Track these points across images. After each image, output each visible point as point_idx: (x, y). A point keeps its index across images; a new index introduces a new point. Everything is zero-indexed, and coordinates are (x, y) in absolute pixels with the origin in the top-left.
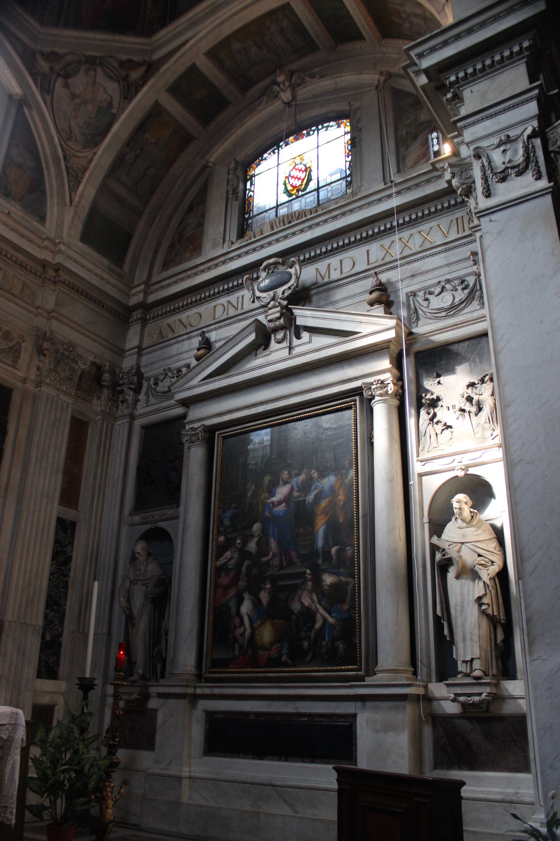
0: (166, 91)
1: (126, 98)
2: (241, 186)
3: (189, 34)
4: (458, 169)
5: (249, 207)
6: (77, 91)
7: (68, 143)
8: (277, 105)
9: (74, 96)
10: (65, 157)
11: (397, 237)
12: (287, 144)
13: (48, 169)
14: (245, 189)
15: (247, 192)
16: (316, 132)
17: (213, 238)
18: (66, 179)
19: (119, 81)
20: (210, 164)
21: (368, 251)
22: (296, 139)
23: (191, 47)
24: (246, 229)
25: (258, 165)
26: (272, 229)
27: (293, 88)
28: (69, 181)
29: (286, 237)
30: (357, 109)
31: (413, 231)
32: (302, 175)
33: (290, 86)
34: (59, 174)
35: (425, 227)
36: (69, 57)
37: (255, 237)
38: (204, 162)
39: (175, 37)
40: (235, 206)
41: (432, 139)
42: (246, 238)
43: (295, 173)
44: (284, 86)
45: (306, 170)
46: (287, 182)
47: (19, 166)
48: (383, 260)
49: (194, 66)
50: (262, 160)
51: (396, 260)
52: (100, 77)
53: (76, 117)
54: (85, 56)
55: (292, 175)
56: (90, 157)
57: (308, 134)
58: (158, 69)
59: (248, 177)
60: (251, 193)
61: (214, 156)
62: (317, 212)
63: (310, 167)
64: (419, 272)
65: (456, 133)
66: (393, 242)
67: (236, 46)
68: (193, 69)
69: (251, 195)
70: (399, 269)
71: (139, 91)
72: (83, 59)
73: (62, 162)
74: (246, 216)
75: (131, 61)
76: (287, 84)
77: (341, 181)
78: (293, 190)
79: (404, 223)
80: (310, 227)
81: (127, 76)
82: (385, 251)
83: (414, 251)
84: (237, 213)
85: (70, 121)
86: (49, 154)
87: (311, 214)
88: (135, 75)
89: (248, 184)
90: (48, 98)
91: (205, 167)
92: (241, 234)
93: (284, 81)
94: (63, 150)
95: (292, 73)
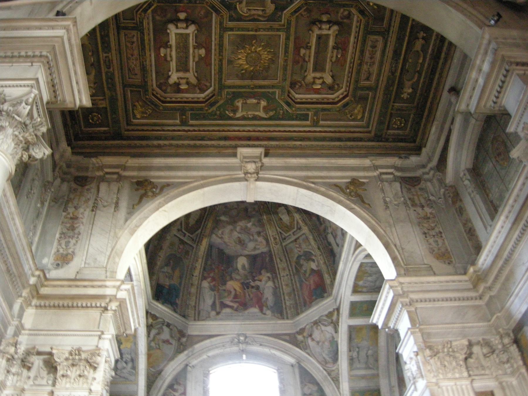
6: (318, 340)
7: (328, 365)
9: (318, 343)
18: (333, 384)
52: (323, 328)
53: (324, 351)
54: (312, 323)
67: (361, 283)
72: (312, 324)
81: (332, 320)
85: (322, 354)
88: (335, 318)
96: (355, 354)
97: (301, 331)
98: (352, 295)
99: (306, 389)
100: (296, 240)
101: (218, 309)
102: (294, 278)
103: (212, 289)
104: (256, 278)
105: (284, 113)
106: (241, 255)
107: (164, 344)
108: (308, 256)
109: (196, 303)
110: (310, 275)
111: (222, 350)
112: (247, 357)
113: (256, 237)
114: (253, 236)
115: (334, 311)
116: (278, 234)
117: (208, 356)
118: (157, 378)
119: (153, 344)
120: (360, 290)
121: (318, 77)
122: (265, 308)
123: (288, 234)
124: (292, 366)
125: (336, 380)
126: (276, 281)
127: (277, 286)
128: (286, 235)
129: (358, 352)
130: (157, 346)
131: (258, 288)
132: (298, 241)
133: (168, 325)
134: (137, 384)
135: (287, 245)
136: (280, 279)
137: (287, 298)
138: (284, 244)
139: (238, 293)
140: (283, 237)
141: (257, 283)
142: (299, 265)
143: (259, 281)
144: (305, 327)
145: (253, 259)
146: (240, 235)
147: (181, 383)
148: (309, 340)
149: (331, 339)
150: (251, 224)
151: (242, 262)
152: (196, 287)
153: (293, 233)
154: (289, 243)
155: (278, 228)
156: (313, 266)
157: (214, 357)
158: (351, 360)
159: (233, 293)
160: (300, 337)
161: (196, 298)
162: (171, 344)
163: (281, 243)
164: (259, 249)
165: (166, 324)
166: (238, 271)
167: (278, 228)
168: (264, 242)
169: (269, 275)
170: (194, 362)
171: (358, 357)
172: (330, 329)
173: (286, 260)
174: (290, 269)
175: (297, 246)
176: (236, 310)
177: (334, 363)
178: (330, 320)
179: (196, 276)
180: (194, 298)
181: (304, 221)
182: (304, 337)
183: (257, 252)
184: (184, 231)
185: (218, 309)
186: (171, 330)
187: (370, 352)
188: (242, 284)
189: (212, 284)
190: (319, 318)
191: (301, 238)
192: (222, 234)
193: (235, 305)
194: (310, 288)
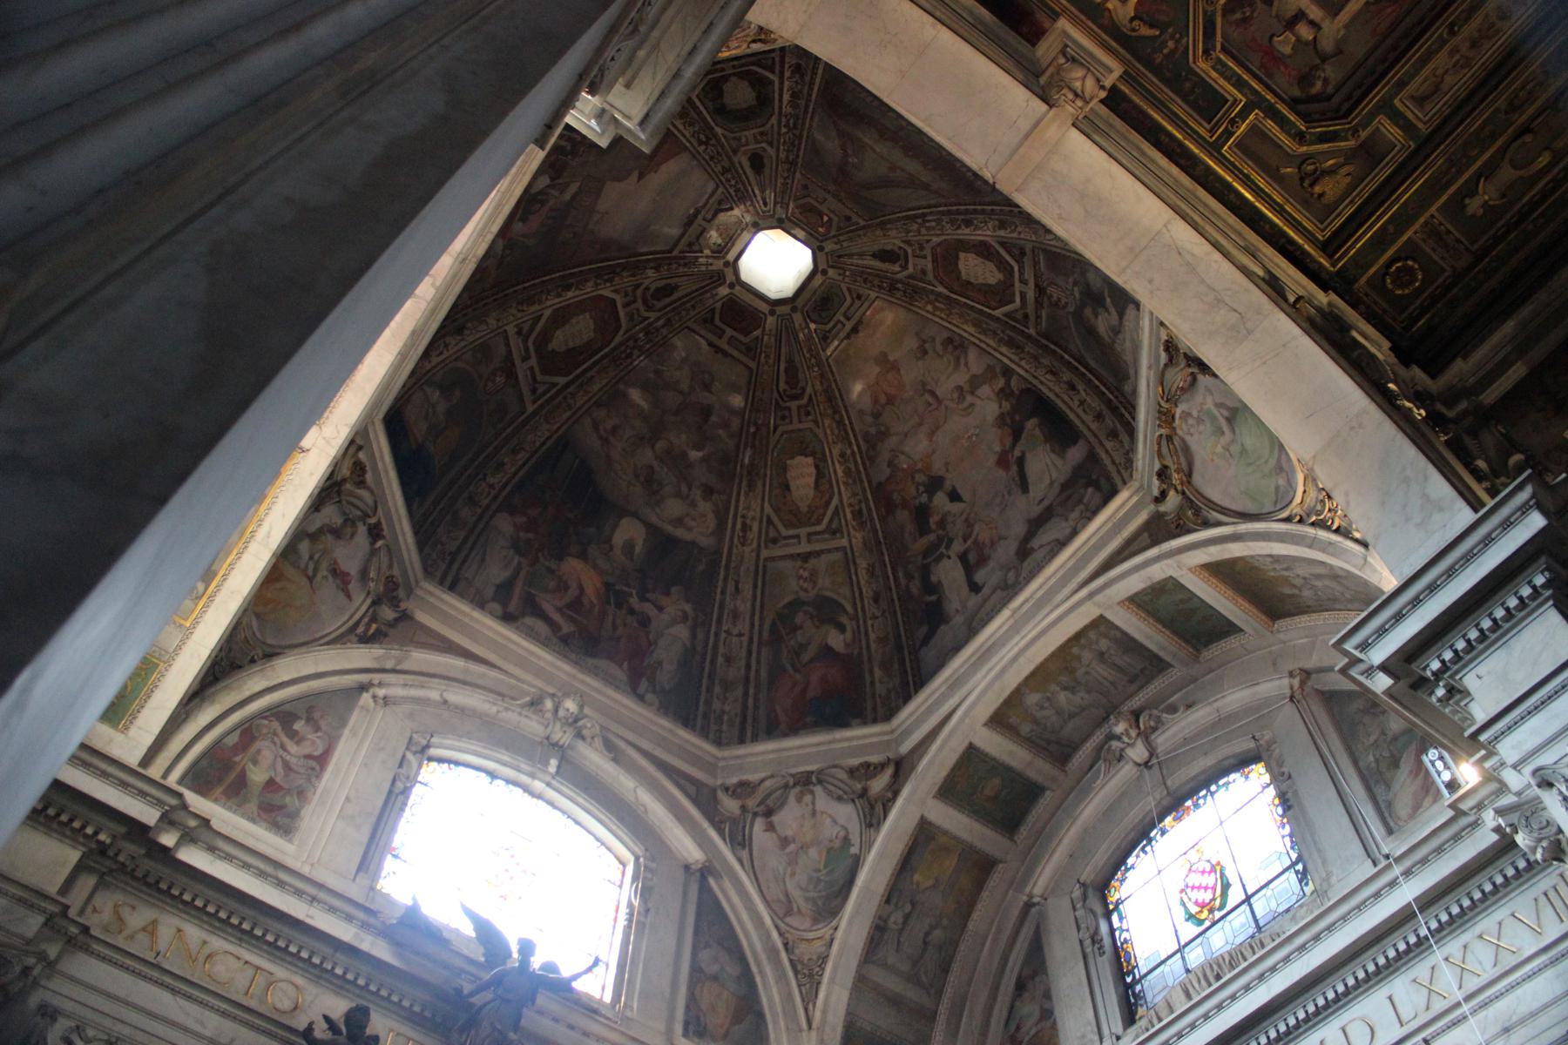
0: (934, 797)
1: (870, 825)
2: (1104, 927)
3: (952, 702)
4: (1518, 814)
5: (1128, 962)
6: (789, 833)
7: (788, 920)
8: (1126, 771)
9: (785, 842)
10: (786, 945)
11: (1437, 955)
12: (1163, 832)
13: (761, 972)
14: (1112, 931)
15: (1117, 933)
16: (1209, 798)
17: (1079, 1034)
19: (853, 801)
20: (1036, 900)
21: (1390, 998)
22: (1178, 819)
23: (961, 720)
24: (1136, 1004)
25: (1122, 881)
26: (1189, 996)
27: (1146, 736)
28: (799, 986)
29: (1220, 1007)
30: (1270, 744)
31: (1466, 937)
32: (1210, 880)
33: (1138, 735)
34: (781, 978)
35: (1487, 923)
36: (768, 783)
37: (1160, 1020)
38: (1025, 898)
39: (930, 711)
40: (1104, 966)
41: (1433, 763)
42: (1143, 1023)
43: (1196, 879)
44: (1130, 737)
45: (1213, 870)
46: (1186, 900)
47: (715, 978)
48: (1428, 1008)
49: (971, 747)
50: (1127, 870)
51: (1458, 1005)
53: (793, 874)
54: (792, 775)
55: (1190, 884)
56: (827, 937)
57: (1196, 806)
58: (913, 768)
59: (1111, 907)
60: (1125, 935)
61: (1040, 884)
62: (1263, 946)
63: (1218, 863)
64: (1515, 1019)
65: (1483, 752)
66: (1433, 968)
67: (1032, 699)
68: (972, 753)
69: (1125, 940)
70: (1472, 1020)
71: (890, 808)
72: (791, 782)
73: (784, 955)
74: (1129, 980)
75: (867, 765)
76: (1133, 733)
77: (1287, 874)
78: (1201, 912)
79: (1441, 927)
80: (1261, 977)
82: (1425, 991)
83: (1486, 978)
84: (1110, 978)
85: (784, 882)
86: (759, 946)
87: (1254, 953)
88: (878, 784)
89: (1115, 917)
90: (745, 854)
91: (1029, 906)
92: (1130, 1018)
93: (1126, 730)
94: (781, 934)
95: (1136, 715)
96: (897, 917)
97: (742, 789)
98: (985, 724)
99: (705, 955)
100: (806, 557)
101: (513, 606)
102: (759, 653)
103: (516, 545)
104: (648, 595)
105: (1173, 52)
106: (635, 515)
107: (331, 579)
108: (827, 612)
109: (459, 549)
110: (811, 661)
111: (494, 709)
112: (559, 767)
113: (697, 494)
114: (690, 489)
115: (882, 766)
116: (761, 521)
117: (445, 702)
118: (253, 661)
119: (304, 547)
120: (1013, 720)
121: (1312, 16)
122: (644, 684)
123: (792, 532)
124: (687, 868)
125: (809, 975)
126: (700, 636)
127: (699, 649)
128: (784, 532)
129: (907, 917)
130: (311, 566)
131: (645, 622)
132: (813, 562)
133: (375, 533)
134: (188, 633)
135: (773, 559)
136: (717, 635)
137: (717, 689)
138: (765, 553)
139: (585, 601)
140: (772, 534)
141: (649, 609)
142: (784, 622)
143: (656, 606)
144: (762, 781)
145: (662, 544)
146: (655, 464)
147: (323, 723)
148: (759, 825)
149: (837, 844)
150: (700, 454)
151: (629, 532)
152: (479, 511)
153: (809, 534)
154: (782, 558)
155: (766, 504)
156: (836, 640)
157: (462, 711)
158: (879, 930)
159: (573, 592)
160: (730, 805)
161: (466, 538)
162: (349, 597)
163: (759, 546)
164: (690, 529)
165: (373, 521)
166: (611, 548)
167: (766, 504)
168: (711, 522)
169: (688, 607)
170: (395, 688)
171: (901, 932)
172: (846, 815)
173: (754, 596)
174: (757, 623)
175: (806, 574)
176: (565, 640)
177: (816, 921)
178: (858, 787)
179: (491, 486)
180: (462, 535)
181: (857, 514)
182: (743, 808)
183: (680, 533)
184: (530, 344)
185: (513, 606)
186: (374, 552)
187: (937, 934)
188: (607, 586)
189: (521, 534)
190: (820, 771)
191: (824, 557)
192: (614, 430)
193: (567, 628)
194: (804, 691)
